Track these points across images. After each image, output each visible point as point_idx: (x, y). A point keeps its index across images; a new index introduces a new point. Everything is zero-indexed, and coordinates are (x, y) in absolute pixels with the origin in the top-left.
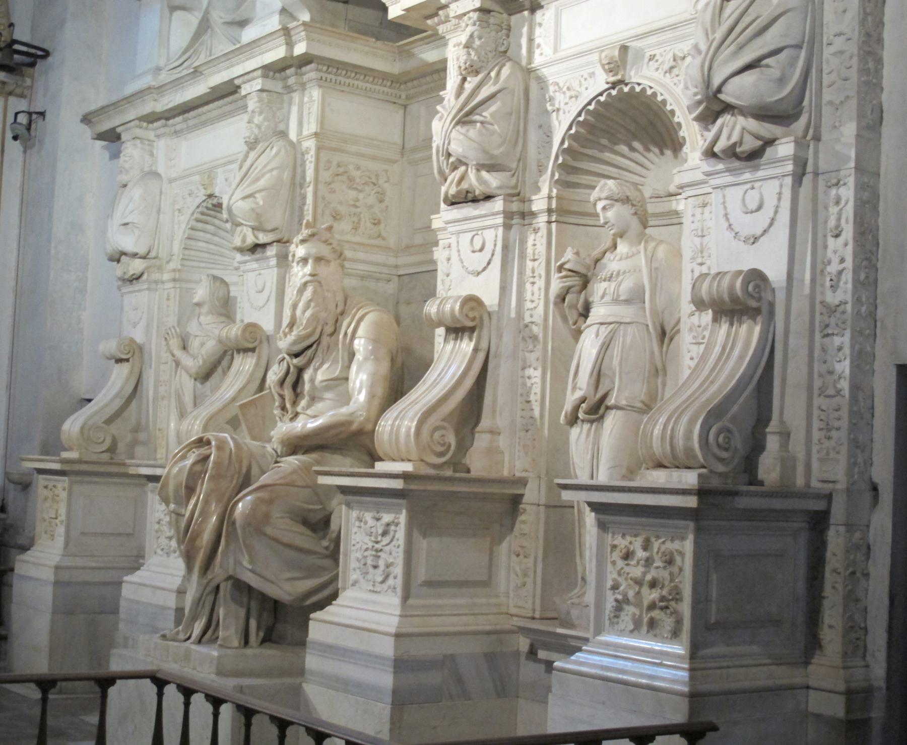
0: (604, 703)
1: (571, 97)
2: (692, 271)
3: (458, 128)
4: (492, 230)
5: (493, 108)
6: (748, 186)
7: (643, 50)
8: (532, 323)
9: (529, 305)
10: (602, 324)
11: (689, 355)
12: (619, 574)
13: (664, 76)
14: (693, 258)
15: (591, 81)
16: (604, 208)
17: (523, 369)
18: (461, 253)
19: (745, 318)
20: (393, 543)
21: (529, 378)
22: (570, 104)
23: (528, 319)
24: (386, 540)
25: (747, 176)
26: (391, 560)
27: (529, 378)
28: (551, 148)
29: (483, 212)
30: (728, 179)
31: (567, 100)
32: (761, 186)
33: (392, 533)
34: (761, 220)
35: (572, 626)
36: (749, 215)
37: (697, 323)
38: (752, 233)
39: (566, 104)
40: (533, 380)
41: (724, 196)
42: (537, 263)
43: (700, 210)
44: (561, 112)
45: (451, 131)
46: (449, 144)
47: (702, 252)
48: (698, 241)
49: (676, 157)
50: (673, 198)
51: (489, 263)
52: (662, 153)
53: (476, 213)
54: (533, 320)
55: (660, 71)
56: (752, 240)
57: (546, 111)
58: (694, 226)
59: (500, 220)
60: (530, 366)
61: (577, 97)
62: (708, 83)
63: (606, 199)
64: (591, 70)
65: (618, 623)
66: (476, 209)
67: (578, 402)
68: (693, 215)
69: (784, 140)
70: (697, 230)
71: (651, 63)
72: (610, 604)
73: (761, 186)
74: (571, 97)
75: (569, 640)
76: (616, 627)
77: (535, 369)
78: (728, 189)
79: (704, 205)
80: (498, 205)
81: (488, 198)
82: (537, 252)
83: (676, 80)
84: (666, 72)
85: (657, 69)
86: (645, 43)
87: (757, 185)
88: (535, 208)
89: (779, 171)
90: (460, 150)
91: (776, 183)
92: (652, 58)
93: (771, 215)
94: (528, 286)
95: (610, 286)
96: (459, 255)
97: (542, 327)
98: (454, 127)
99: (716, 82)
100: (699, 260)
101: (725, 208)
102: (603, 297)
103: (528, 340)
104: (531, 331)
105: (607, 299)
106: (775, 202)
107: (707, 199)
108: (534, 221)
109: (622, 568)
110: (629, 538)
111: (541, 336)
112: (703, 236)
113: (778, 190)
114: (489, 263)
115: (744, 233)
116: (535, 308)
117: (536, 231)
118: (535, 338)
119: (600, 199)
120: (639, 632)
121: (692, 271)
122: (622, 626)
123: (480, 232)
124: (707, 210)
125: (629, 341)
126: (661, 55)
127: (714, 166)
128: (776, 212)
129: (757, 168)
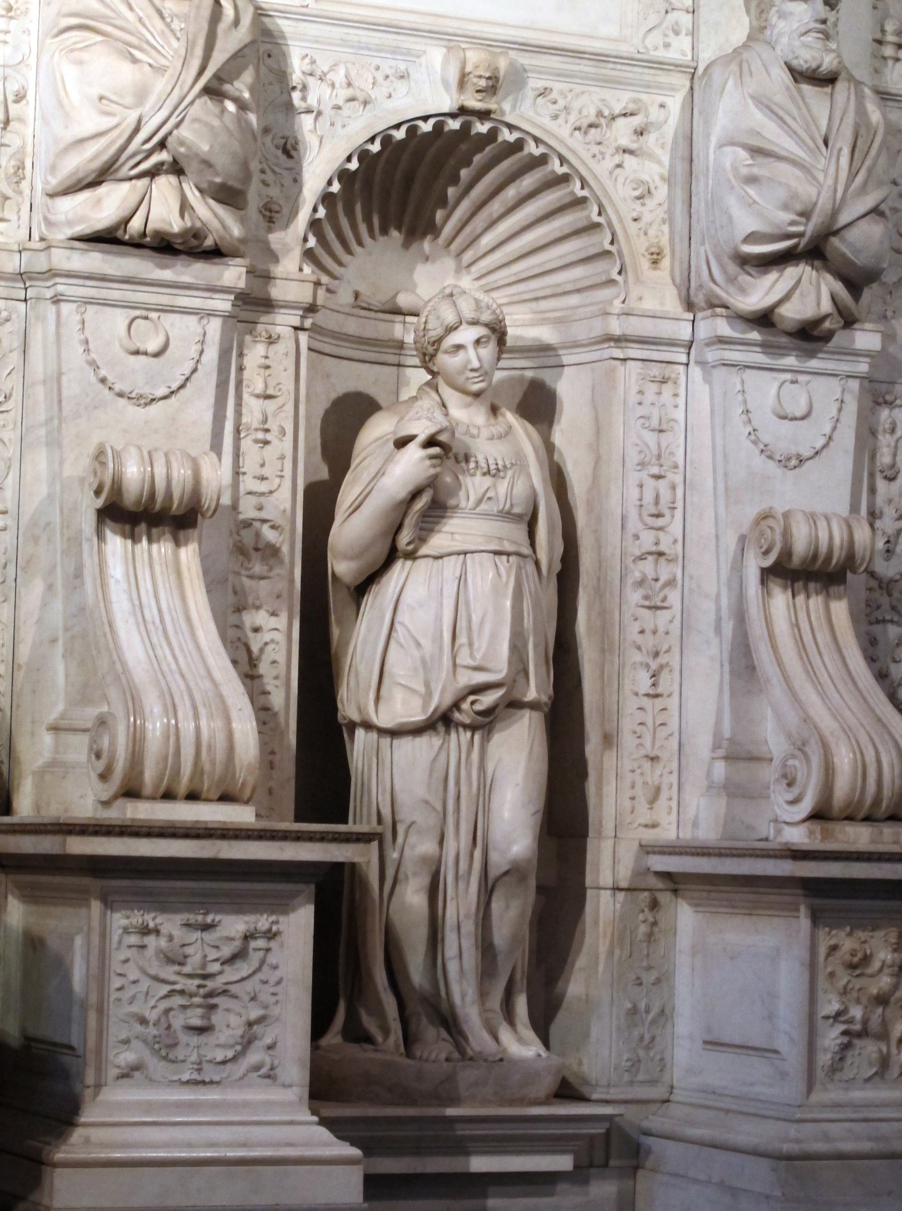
0: (890, 1193)
1: (352, 99)
2: (641, 486)
3: (205, 98)
4: (193, 319)
5: (248, 77)
6: (788, 376)
7: (525, 70)
8: (264, 521)
9: (248, 483)
10: (497, 553)
11: (636, 627)
12: (845, 992)
13: (572, 135)
14: (642, 465)
15: (401, 87)
16: (478, 342)
17: (239, 609)
18: (91, 346)
19: (812, 586)
20: (260, 976)
21: (256, 630)
22: (345, 112)
23: (248, 510)
24: (244, 969)
25: (791, 361)
26: (255, 1013)
27: (256, 630)
28: (297, 181)
29: (186, 279)
30: (758, 357)
31: (340, 102)
32: (808, 382)
33: (255, 958)
34: (808, 437)
35: (455, 1101)
36: (786, 422)
37: (651, 574)
38: (794, 450)
39: (338, 108)
40: (267, 637)
41: (743, 382)
42: (271, 406)
43: (654, 387)
44: (325, 121)
45: (192, 103)
46: (177, 125)
47: (659, 457)
48: (651, 438)
49: (406, 245)
50: (400, 318)
51: (182, 386)
52: (384, 231)
53: (167, 275)
54: (264, 515)
55: (561, 120)
56: (794, 462)
57: (289, 107)
58: (641, 411)
59: (224, 304)
60: (258, 608)
61: (365, 103)
62: (835, 214)
63: (486, 325)
64: (402, 66)
65: (842, 1069)
66: (163, 267)
67: (465, 692)
68: (641, 392)
69: (868, 326)
70: (647, 418)
71: (540, 99)
72: (831, 1037)
73: (808, 382)
74: (352, 99)
75: (458, 1126)
76: (838, 1076)
77: (274, 614)
78: (748, 371)
79: (664, 381)
80: (233, 274)
81: (216, 253)
82: (272, 382)
83: (595, 149)
84: (578, 129)
85: (555, 117)
86: (534, 62)
87: (802, 378)
88: (277, 292)
89: (844, 367)
90: (205, 147)
91: (835, 385)
92: (543, 93)
93: (827, 429)
94: (247, 444)
95: (495, 485)
96: (87, 351)
97: (287, 534)
98: (199, 96)
99: (844, 219)
100: (655, 470)
101: (745, 402)
102: (479, 502)
103: (252, 552)
104: (258, 535)
105: (484, 507)
106: (834, 412)
107: (669, 370)
108: (264, 319)
109: (849, 982)
110: (862, 935)
111: (285, 549)
112: (661, 431)
113: (838, 395)
114: (182, 386)
115: (782, 447)
116: (271, 492)
117: (271, 340)
118: (271, 552)
119: (474, 323)
120: (883, 1078)
121: (641, 486)
122: (848, 1073)
123: (154, 315)
124: (667, 389)
125: (533, 589)
126: (561, 93)
127: (743, 332)
128: (834, 429)
129: (812, 354)
